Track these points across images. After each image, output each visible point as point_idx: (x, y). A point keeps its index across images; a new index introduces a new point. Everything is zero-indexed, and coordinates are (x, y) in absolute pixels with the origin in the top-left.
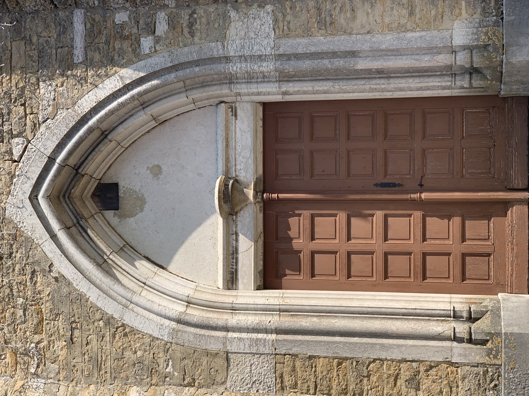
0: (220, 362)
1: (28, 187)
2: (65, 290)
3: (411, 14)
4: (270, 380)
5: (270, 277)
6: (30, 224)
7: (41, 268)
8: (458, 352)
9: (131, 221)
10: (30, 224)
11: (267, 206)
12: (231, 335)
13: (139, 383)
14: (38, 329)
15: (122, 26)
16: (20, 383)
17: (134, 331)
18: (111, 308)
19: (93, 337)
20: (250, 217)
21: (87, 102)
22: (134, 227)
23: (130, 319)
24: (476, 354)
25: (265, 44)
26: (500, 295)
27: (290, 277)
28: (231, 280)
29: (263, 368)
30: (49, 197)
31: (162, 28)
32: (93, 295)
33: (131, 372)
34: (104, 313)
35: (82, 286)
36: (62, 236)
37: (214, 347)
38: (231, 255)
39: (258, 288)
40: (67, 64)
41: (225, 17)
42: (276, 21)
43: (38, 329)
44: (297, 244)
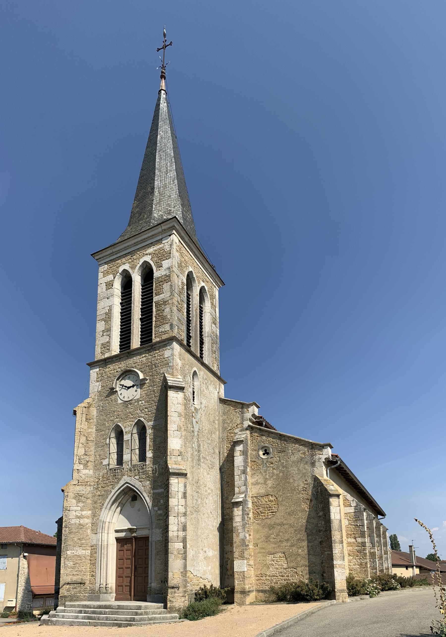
0: (95, 532)
1: (129, 481)
2: (109, 493)
3: (158, 573)
4: (93, 544)
5: (118, 540)
6: (122, 482)
7: (113, 486)
8: (97, 585)
9: (129, 505)
10: (122, 482)
11: (131, 538)
12: (101, 534)
13: (92, 513)
14: (102, 487)
15: (160, 502)
16: (92, 484)
17: (101, 510)
18: (105, 505)
19: (100, 501)
20: (129, 535)
21: (145, 495)
22: (128, 505)
23: (103, 509)
24: (97, 589)
25: (154, 539)
26: (115, 595)
27: (119, 545)
28: (117, 531)
29: (94, 542)
30: (127, 486)
31: (159, 512)
32: (108, 500)
33: (94, 511)
34: (104, 503)
35: (109, 498)
36: (119, 491)
37: (98, 530)
38: (121, 531)
39: (116, 538)
40: (153, 488)
41: (160, 528)
42: (159, 541)
43: (102, 487)
44: (125, 546)
